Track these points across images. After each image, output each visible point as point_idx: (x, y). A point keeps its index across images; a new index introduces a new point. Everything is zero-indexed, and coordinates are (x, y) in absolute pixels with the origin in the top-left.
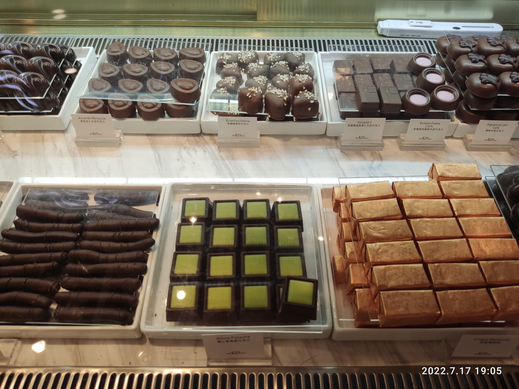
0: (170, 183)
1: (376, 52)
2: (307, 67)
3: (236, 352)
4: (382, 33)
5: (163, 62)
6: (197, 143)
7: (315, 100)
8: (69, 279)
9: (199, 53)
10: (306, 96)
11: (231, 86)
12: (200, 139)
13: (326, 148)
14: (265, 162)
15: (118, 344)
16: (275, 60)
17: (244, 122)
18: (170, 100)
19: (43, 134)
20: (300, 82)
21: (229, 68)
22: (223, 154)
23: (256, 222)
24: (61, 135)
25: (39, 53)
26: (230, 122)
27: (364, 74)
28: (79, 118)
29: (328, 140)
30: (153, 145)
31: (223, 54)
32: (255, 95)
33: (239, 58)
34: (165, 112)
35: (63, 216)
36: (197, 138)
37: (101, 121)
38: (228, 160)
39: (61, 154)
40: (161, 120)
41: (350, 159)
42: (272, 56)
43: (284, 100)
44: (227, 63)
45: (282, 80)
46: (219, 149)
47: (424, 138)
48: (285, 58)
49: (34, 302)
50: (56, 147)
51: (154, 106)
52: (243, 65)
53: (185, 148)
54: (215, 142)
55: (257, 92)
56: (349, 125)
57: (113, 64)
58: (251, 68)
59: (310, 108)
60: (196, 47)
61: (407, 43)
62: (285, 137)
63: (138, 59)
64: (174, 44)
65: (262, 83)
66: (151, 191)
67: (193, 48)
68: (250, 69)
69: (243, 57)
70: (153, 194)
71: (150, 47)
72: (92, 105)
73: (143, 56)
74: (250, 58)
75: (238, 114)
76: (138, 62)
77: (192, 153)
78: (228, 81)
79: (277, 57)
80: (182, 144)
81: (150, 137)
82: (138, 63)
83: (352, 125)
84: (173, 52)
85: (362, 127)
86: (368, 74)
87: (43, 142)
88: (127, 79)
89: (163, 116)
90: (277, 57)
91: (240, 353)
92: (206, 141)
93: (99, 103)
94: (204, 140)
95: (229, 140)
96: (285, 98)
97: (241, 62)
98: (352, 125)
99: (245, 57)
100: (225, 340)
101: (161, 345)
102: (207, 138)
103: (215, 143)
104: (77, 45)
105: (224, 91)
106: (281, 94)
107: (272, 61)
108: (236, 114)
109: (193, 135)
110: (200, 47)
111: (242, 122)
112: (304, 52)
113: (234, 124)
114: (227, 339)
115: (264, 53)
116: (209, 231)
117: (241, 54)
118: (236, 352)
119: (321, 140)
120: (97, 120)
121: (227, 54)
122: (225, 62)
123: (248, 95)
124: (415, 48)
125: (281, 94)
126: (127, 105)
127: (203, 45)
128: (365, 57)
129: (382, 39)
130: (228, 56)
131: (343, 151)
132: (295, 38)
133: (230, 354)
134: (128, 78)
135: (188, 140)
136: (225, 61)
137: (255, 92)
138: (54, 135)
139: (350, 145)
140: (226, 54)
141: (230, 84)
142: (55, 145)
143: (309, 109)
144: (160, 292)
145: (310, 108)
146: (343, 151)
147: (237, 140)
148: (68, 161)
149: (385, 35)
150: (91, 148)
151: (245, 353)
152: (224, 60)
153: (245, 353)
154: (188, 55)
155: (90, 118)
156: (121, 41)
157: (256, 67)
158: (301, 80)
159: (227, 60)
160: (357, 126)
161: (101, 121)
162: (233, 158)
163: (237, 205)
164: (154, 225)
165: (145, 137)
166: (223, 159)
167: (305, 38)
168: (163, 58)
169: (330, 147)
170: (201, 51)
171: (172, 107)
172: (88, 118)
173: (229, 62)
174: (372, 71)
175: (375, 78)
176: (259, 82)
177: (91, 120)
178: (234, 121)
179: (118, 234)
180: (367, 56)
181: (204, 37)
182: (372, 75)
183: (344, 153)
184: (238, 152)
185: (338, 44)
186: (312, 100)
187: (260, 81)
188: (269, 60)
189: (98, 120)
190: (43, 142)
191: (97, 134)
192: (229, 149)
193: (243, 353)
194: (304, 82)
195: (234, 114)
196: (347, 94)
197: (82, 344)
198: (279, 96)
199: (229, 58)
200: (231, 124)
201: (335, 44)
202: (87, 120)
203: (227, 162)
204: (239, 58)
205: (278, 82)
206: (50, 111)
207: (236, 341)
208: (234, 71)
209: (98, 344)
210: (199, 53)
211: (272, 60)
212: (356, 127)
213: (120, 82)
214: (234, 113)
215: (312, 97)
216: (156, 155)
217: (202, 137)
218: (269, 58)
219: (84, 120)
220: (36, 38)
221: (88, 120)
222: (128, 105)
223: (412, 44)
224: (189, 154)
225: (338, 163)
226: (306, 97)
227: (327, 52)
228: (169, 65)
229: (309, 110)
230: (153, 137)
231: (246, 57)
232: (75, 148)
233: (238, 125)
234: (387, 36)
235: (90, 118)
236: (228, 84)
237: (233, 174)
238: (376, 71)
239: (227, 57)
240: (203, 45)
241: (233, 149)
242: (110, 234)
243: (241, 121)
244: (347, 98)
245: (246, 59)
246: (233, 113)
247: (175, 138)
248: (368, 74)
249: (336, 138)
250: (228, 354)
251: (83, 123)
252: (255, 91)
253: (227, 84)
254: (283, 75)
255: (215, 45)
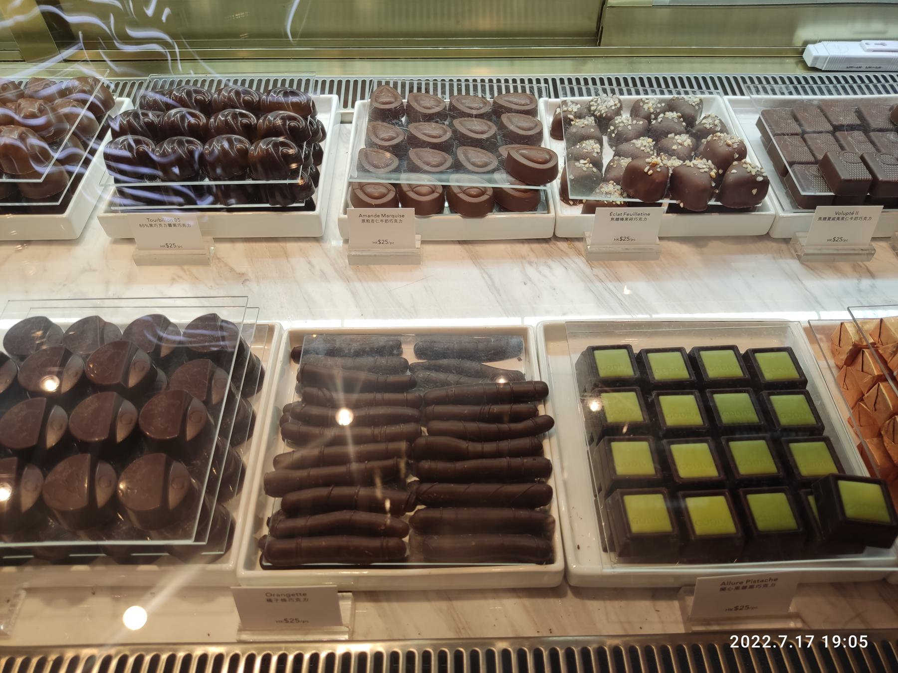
0: (541, 322)
1: (827, 97)
2: (717, 122)
3: (743, 607)
4: (816, 64)
5: (477, 119)
6: (549, 255)
7: (763, 177)
8: (501, 487)
9: (528, 102)
10: (749, 170)
11: (596, 156)
12: (551, 247)
13: (774, 258)
14: (677, 285)
15: (519, 597)
16: (656, 111)
17: (640, 216)
18: (504, 181)
19: (283, 244)
20: (729, 145)
21: (583, 125)
22: (600, 272)
23: (675, 387)
24: (314, 245)
25: (228, 104)
26: (615, 217)
27: (821, 132)
28: (360, 216)
29: (774, 244)
30: (475, 259)
31: (564, 103)
32: (659, 170)
33: (593, 108)
34: (446, 204)
35: (386, 380)
36: (545, 245)
37: (395, 219)
38: (610, 281)
39: (324, 276)
40: (436, 218)
41: (820, 276)
42: (650, 105)
43: (711, 177)
44: (576, 117)
45: (681, 144)
46: (589, 263)
47: (836, 239)
48: (671, 106)
49: (383, 528)
50: (313, 266)
51: (483, 192)
52: (603, 122)
53: (530, 263)
54: (578, 252)
55: (661, 164)
56: (820, 219)
57: (393, 124)
58: (621, 125)
59: (756, 189)
60: (466, 94)
61: (813, 81)
62: (697, 241)
63: (433, 114)
64: (483, 87)
65: (649, 150)
66: (510, 337)
67: (508, 94)
68: (619, 126)
69: (601, 108)
70: (514, 341)
71: (443, 93)
72: (376, 195)
73: (438, 108)
74: (613, 108)
75: (622, 203)
76: (433, 119)
77: (545, 271)
78: (589, 148)
79: (659, 105)
80: (523, 257)
81: (466, 246)
82: (434, 121)
83: (825, 219)
84: (439, 102)
85: (840, 221)
86: (828, 132)
87: (287, 257)
88: (424, 149)
89: (440, 210)
90: (659, 105)
91: (748, 608)
92: (562, 250)
93: (389, 191)
94: (559, 248)
95: (604, 247)
96: (713, 173)
97: (598, 115)
98: (825, 219)
99: (604, 107)
100: (734, 587)
101: (594, 598)
102: (563, 245)
103: (579, 253)
104: (308, 90)
105: (588, 164)
106: (704, 166)
107: (653, 113)
108: (619, 203)
109: (546, 241)
110: (528, 91)
111: (637, 216)
112: (702, 96)
113: (622, 219)
114: (738, 585)
115: (630, 100)
116: (653, 401)
117: (596, 102)
118: (743, 607)
119: (760, 245)
120: (389, 218)
121: (573, 102)
122: (571, 117)
123: (646, 170)
124: (803, 88)
125: (704, 166)
126: (437, 192)
127: (531, 89)
128: (812, 105)
129: (816, 75)
130: (576, 106)
131: (805, 263)
132: (670, 73)
133: (731, 610)
134: (426, 147)
135: (532, 249)
136: (571, 114)
137: (658, 164)
138: (302, 245)
139: (817, 252)
140: (574, 103)
141: (594, 153)
142: (310, 263)
143: (754, 191)
144: (573, 508)
145: (756, 189)
146: (805, 263)
147: (620, 247)
148: (338, 288)
149: (820, 68)
150: (372, 266)
151: (756, 608)
152: (570, 112)
153: (756, 608)
154: (514, 107)
155: (378, 216)
156: (391, 85)
157: (630, 123)
158: (730, 142)
159: (575, 112)
160: (834, 219)
161: (396, 221)
162: (617, 278)
163: (685, 358)
164: (541, 393)
165: (458, 247)
166: (601, 280)
167: (640, 74)
168: (474, 112)
169: (781, 256)
170: (533, 101)
171: (512, 193)
172: (376, 216)
173: (579, 116)
174: (831, 128)
175: (808, 140)
176: (642, 148)
177: (381, 218)
178: (623, 215)
179: (487, 408)
180: (815, 103)
181: (365, 76)
182: (833, 133)
183: (807, 266)
184: (623, 268)
185: (761, 84)
186: (759, 175)
187: (645, 146)
188: (646, 110)
189: (391, 218)
190: (287, 257)
191: (172, 246)
192: (606, 262)
193: (752, 608)
194: (735, 146)
195: (614, 203)
196: (804, 166)
197: (457, 599)
198: (702, 171)
199: (578, 109)
200: (617, 219)
201: (604, 85)
202: (374, 218)
203: (610, 285)
204: (593, 108)
205: (675, 147)
206: (303, 205)
207: (752, 587)
208: (592, 130)
209: (485, 598)
210: (528, 102)
211: (652, 110)
212: (831, 222)
213: (412, 153)
214: (615, 202)
215: (758, 171)
216: (486, 276)
217: (555, 244)
218: (646, 107)
219: (368, 218)
220: (212, 81)
221: (374, 219)
222: (438, 193)
223: (814, 82)
224: (540, 273)
225: (802, 283)
226: (749, 171)
227: (746, 97)
228: (487, 124)
229: (754, 194)
230: (470, 247)
231: (606, 106)
232: (346, 267)
233: (628, 221)
234: (823, 69)
235: (378, 216)
236: (590, 153)
237: (626, 306)
238: (837, 128)
239: (575, 108)
240: (531, 89)
241: (614, 263)
242: (466, 409)
243: (636, 214)
244: (806, 172)
245: (607, 110)
246: (613, 201)
247: (508, 247)
248: (828, 132)
249: (786, 241)
250: (729, 610)
251: (366, 223)
252: (658, 163)
253: (587, 152)
254: (680, 135)
255: (555, 87)
